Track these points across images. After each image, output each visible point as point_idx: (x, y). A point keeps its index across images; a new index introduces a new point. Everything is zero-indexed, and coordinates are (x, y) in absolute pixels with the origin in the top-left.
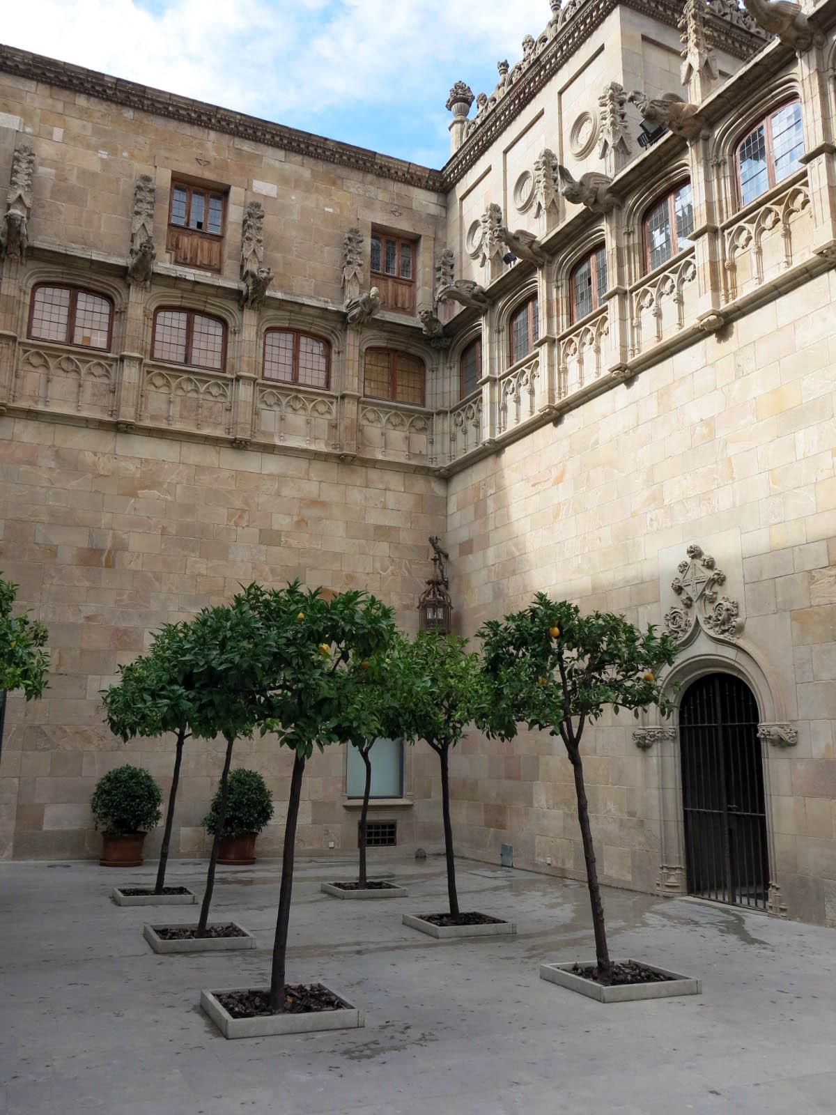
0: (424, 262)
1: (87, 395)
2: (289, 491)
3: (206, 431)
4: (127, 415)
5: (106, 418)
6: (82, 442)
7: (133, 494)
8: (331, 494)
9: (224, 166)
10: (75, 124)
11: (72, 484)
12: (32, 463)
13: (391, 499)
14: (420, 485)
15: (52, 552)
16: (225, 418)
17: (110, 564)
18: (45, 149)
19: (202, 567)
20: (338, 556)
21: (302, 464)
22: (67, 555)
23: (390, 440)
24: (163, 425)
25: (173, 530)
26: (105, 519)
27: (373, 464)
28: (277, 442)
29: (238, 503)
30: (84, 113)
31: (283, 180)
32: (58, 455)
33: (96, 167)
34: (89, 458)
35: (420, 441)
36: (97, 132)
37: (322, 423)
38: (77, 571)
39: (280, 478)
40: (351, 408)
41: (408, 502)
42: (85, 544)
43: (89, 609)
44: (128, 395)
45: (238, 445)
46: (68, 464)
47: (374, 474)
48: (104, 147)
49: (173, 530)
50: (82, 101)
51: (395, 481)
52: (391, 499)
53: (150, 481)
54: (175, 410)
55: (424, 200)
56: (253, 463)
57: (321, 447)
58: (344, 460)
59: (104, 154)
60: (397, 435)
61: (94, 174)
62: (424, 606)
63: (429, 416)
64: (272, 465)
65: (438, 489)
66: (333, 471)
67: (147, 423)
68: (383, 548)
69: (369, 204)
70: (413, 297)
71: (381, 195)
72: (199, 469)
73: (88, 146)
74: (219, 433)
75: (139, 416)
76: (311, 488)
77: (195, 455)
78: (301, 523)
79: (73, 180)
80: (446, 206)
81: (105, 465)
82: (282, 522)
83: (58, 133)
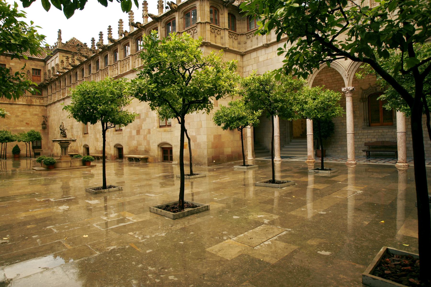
0: (42, 73)
2: (20, 110)
8: (27, 110)
9: (4, 61)
13: (37, 110)
14: (42, 107)
19: (6, 121)
20: (28, 118)
21: (22, 106)
23: (36, 101)
27: (34, 105)
28: (17, 103)
29: (12, 112)
31: (15, 63)
35: (42, 101)
37: (25, 100)
39: (19, 108)
40: (29, 98)
41: (40, 110)
47: (34, 107)
51: (38, 107)
52: (37, 110)
55: (42, 63)
56: (14, 106)
57: (25, 103)
58: (29, 105)
60: (38, 101)
62: (42, 125)
63: (43, 98)
64: (17, 106)
65: (45, 108)
66: (27, 106)
68: (36, 117)
69: (31, 65)
70: (40, 79)
71: (34, 63)
76: (24, 109)
78: (22, 114)
80: (45, 64)
82: (19, 114)
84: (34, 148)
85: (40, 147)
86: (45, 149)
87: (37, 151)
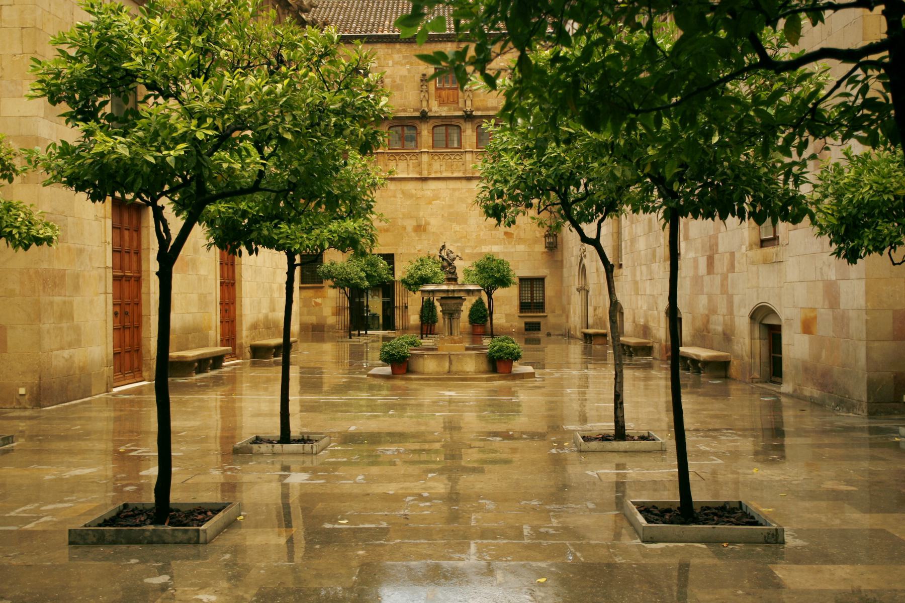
1: (411, 168)
3: (454, 175)
4: (425, 175)
5: (418, 176)
6: (411, 186)
7: (430, 203)
10: (396, 57)
11: (408, 203)
12: (395, 197)
15: (404, 228)
16: (462, 168)
17: (425, 230)
18: (388, 71)
22: (410, 229)
24: (439, 175)
25: (446, 215)
26: (421, 214)
30: (399, 52)
32: (403, 193)
33: (405, 73)
34: (414, 192)
36: (404, 57)
38: (413, 234)
42: (415, 224)
43: (419, 247)
44: (425, 166)
45: (469, 179)
46: (407, 195)
48: (408, 63)
49: (446, 215)
50: (398, 46)
53: (436, 197)
54: (444, 168)
59: (408, 67)
61: (405, 76)
67: (433, 175)
72: (454, 190)
73: (402, 65)
74: (460, 175)
75: (429, 173)
77: (452, 184)
79: (398, 81)
81: (419, 194)
83: (390, 63)
84: (524, 307)
85: (540, 306)
86: (553, 312)
87: (533, 317)
